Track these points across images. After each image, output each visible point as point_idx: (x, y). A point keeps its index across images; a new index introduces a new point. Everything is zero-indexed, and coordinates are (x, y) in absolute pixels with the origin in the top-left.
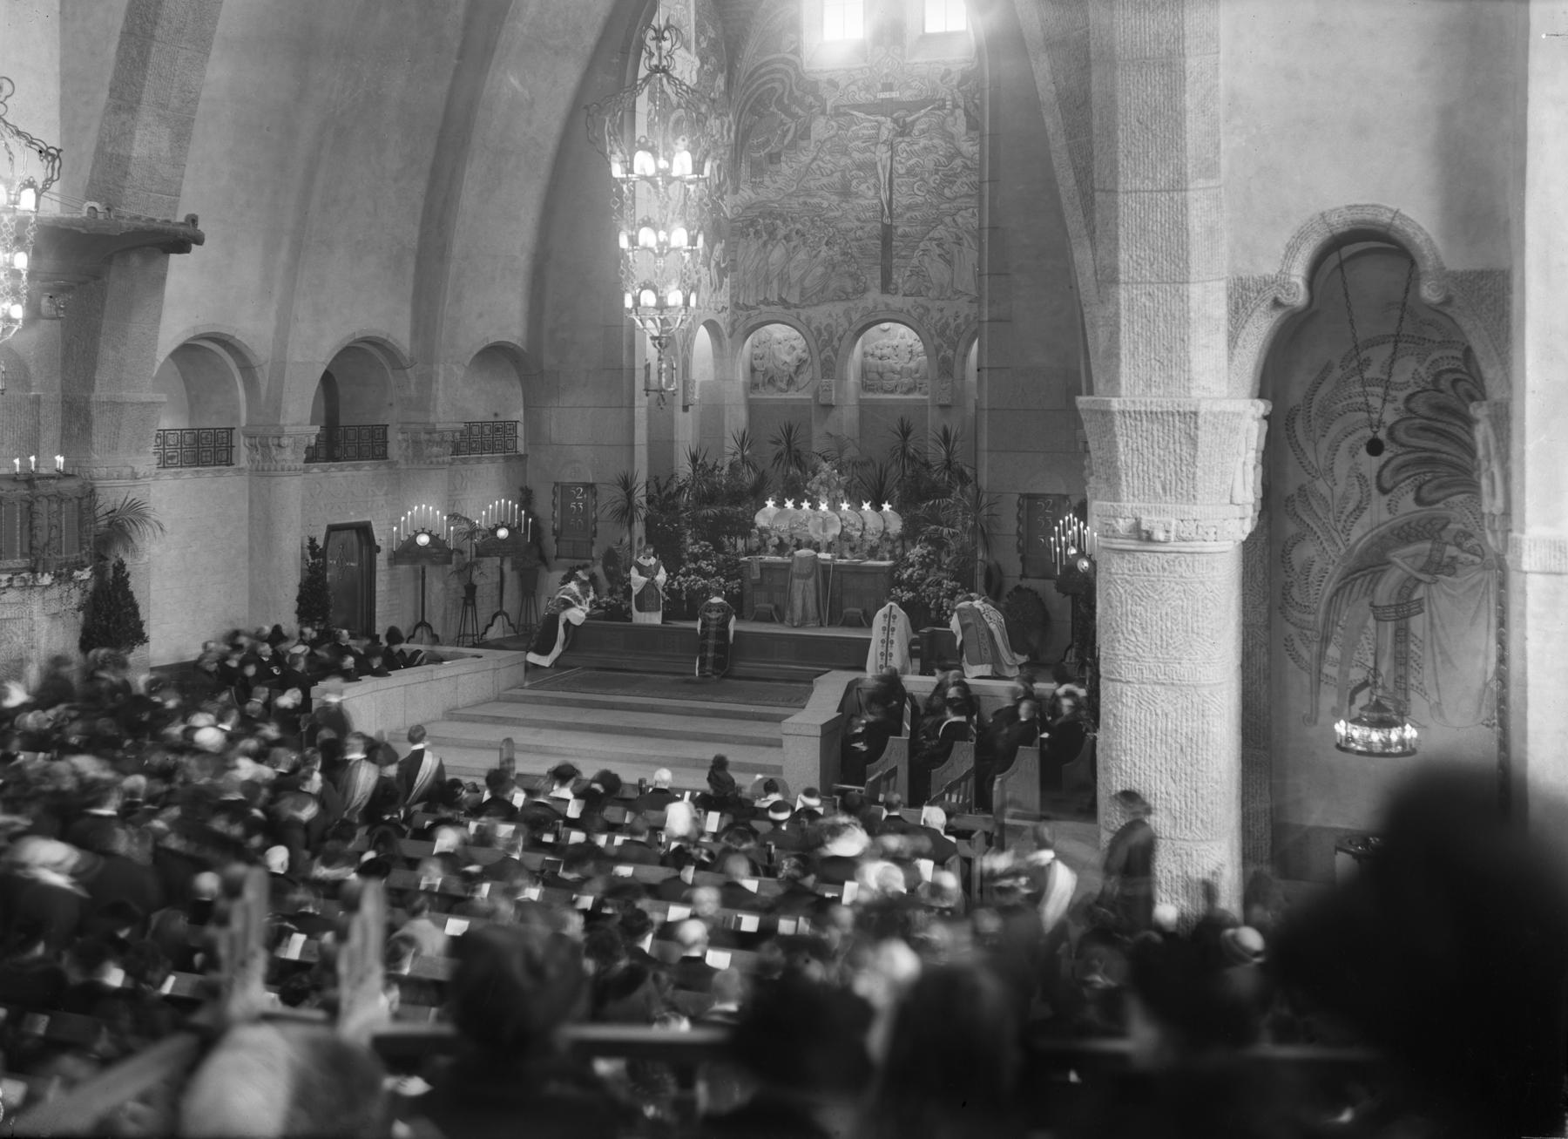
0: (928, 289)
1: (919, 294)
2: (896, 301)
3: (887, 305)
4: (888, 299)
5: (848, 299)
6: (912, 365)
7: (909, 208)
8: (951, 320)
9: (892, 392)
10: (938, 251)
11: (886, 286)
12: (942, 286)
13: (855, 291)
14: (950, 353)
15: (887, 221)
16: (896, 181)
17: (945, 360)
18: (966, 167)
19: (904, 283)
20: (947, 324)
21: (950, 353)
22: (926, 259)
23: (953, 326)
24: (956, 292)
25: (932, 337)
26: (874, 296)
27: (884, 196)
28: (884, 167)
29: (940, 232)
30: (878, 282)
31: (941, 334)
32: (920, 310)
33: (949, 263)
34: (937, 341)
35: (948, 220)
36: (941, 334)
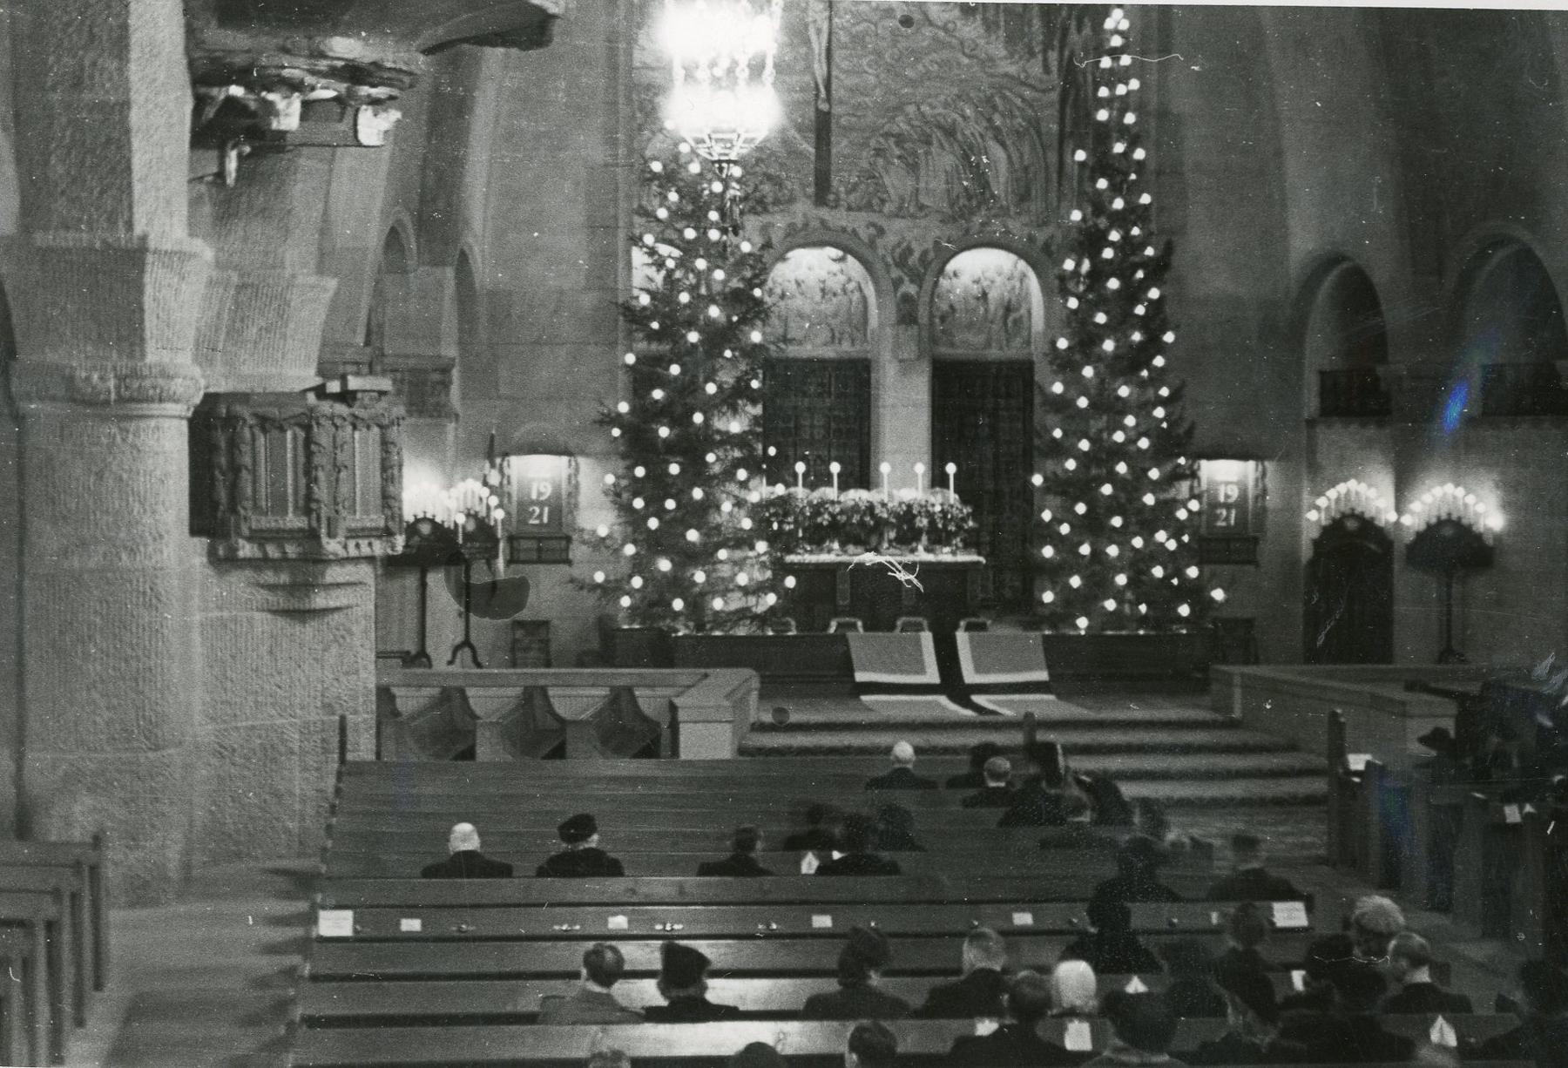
0: (883, 201)
1: (869, 207)
2: (839, 218)
3: (823, 222)
4: (824, 213)
5: (766, 210)
6: (827, 307)
7: (852, 90)
8: (914, 245)
9: (800, 343)
10: (897, 152)
11: (822, 192)
12: (902, 200)
13: (776, 202)
14: (911, 289)
15: (824, 107)
16: (838, 55)
17: (907, 298)
18: (935, 39)
19: (848, 192)
20: (909, 251)
21: (911, 289)
22: (880, 161)
23: (917, 255)
24: (921, 207)
25: (887, 265)
26: (803, 209)
27: (820, 70)
28: (819, 31)
29: (901, 125)
30: (811, 190)
31: (901, 262)
32: (872, 231)
33: (913, 168)
34: (896, 273)
35: (911, 109)
36: (901, 262)
